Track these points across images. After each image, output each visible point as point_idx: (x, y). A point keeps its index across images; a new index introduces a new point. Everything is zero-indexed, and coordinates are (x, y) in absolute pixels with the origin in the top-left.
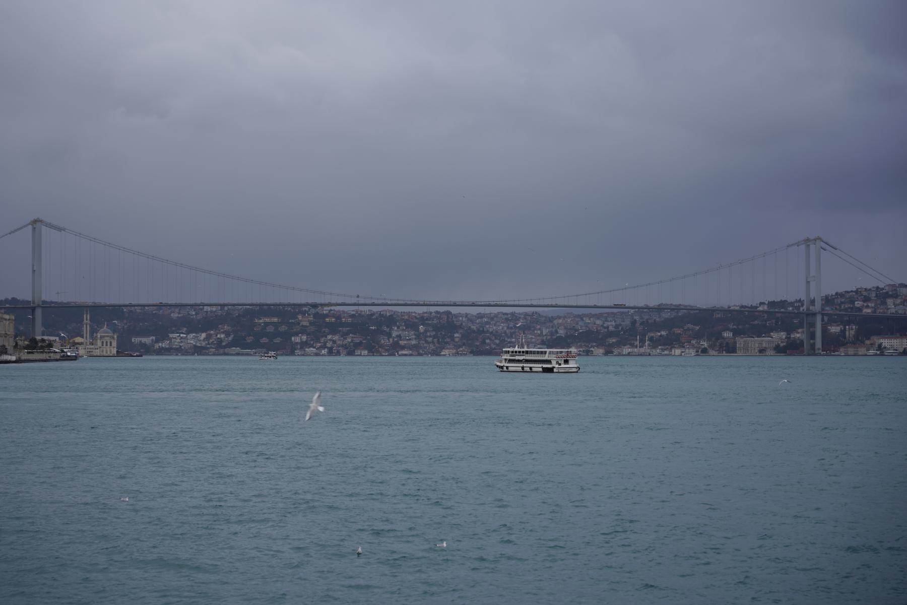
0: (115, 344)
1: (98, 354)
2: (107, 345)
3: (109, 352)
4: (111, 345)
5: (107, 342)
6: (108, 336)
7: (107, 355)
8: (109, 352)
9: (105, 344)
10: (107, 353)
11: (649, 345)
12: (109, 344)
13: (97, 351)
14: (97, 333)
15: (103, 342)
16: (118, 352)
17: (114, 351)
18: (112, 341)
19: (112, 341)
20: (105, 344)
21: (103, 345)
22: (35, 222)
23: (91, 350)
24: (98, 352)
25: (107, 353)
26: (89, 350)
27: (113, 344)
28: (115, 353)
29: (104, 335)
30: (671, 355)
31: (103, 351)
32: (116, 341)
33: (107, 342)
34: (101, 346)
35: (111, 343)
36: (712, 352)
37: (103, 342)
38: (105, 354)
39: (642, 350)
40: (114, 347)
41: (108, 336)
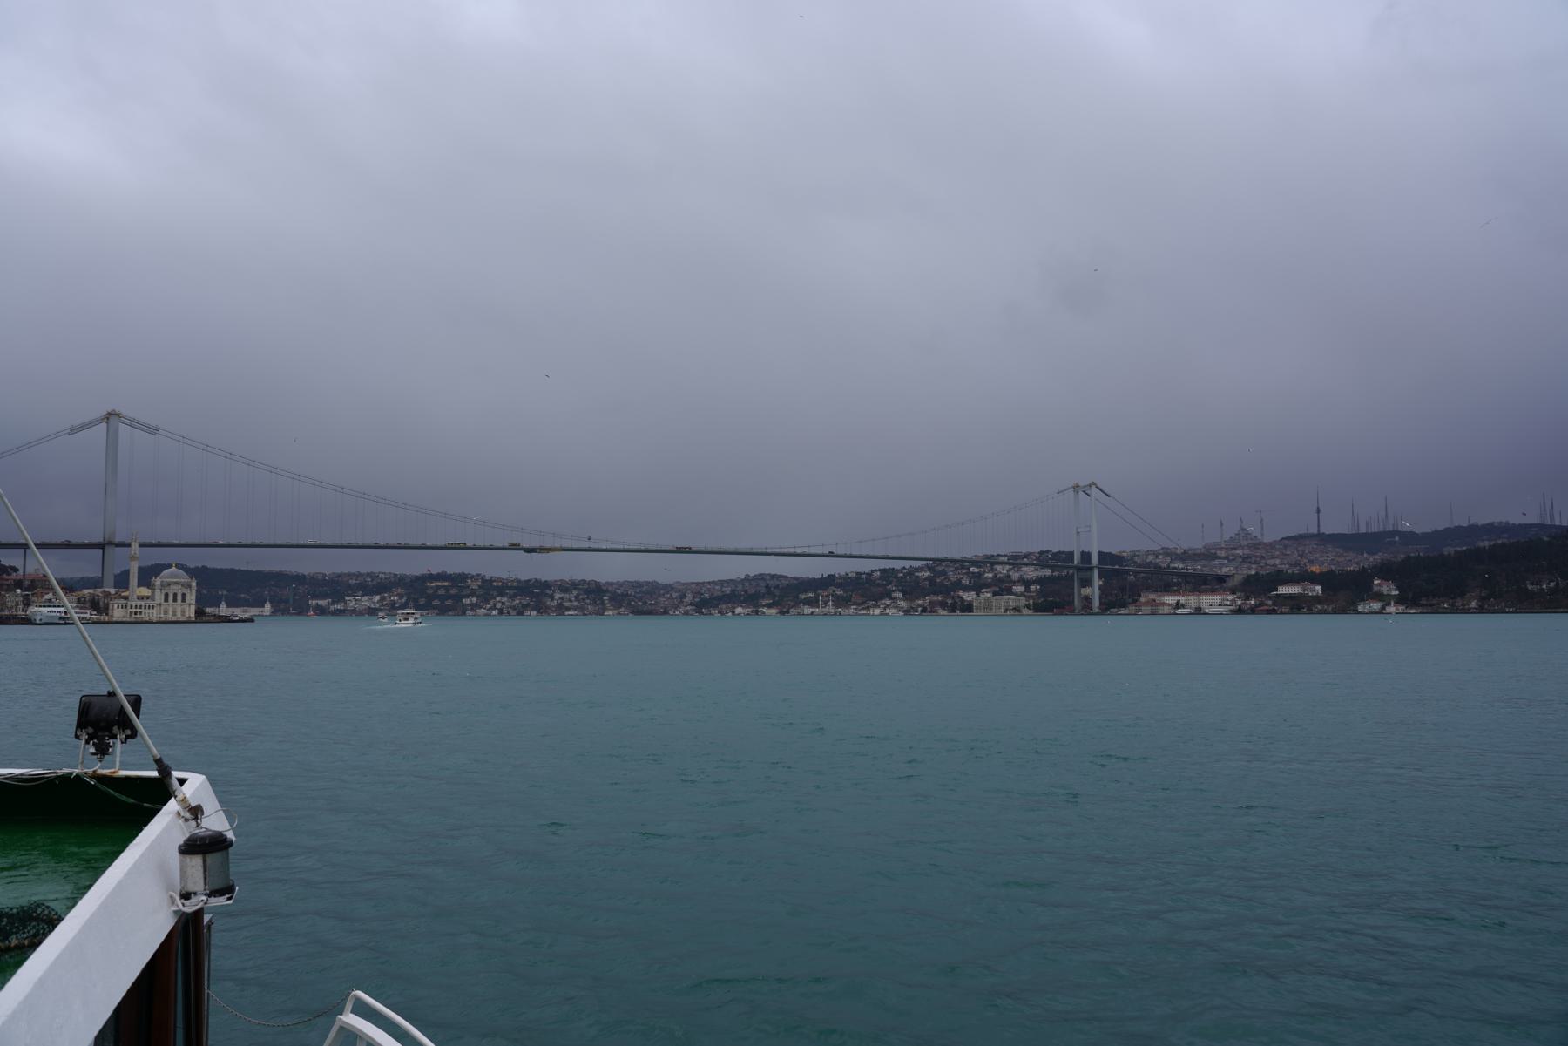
0: (194, 597)
1: (154, 618)
2: (175, 600)
3: (179, 615)
4: (184, 600)
5: (175, 595)
6: (177, 583)
7: (174, 619)
8: (179, 615)
11: (833, 605)
12: (179, 598)
13: (151, 611)
14: (156, 577)
15: (167, 596)
16: (200, 613)
17: (191, 612)
18: (187, 592)
19: (187, 592)
21: (166, 599)
22: (109, 416)
23: (138, 610)
24: (154, 614)
25: (174, 613)
26: (134, 610)
27: (188, 598)
28: (193, 615)
30: (869, 614)
31: (166, 612)
32: (194, 592)
33: (175, 595)
34: (162, 601)
35: (184, 596)
36: (1026, 611)
37: (167, 596)
38: (170, 617)
39: (826, 610)
40: (190, 604)
41: (177, 583)
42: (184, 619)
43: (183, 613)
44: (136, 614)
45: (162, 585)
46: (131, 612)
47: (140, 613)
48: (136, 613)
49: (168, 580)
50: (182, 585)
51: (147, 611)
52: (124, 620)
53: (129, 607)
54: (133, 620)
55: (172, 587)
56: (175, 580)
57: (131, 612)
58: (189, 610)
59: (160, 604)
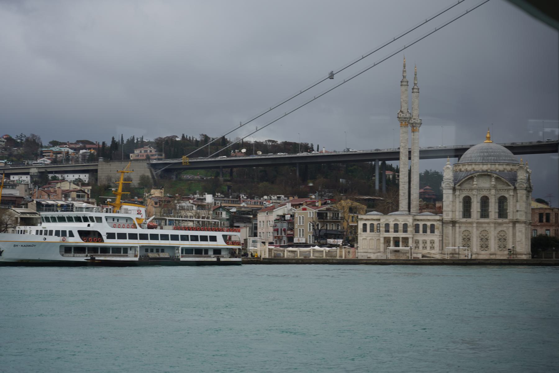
1: (436, 254)
2: (484, 213)
3: (493, 245)
7: (484, 255)
8: (493, 245)
9: (476, 207)
10: (485, 246)
12: (493, 208)
13: (429, 237)
15: (467, 202)
20: (476, 207)
21: (467, 212)
23: (401, 235)
25: (485, 246)
26: (392, 235)
29: (478, 168)
31: (467, 241)
34: (458, 215)
37: (467, 202)
40: (515, 223)
41: (486, 175)
42: (503, 255)
43: (502, 240)
44: (397, 244)
45: (456, 180)
46: (387, 241)
47: (406, 240)
48: (397, 244)
49: (469, 168)
50: (497, 179)
51: (421, 237)
52: (373, 257)
53: (382, 229)
54: (390, 257)
55: (475, 182)
56: (485, 167)
57: (387, 241)
58: (514, 235)
59: (454, 223)
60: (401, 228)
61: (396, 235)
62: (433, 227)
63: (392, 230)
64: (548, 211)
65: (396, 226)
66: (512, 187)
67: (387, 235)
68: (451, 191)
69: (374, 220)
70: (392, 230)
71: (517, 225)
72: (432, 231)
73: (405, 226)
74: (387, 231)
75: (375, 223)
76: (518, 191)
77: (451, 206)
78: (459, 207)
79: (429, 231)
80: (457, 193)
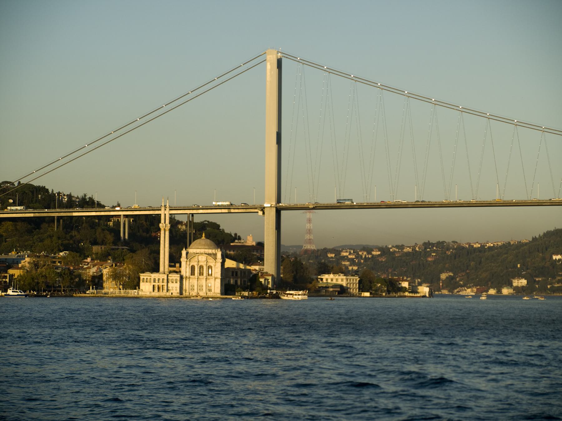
2: (201, 274)
15: (193, 268)
21: (193, 273)
26: (156, 284)
34: (188, 274)
37: (193, 268)
53: (152, 281)
60: (161, 280)
61: (159, 284)
62: (176, 280)
63: (157, 281)
64: (236, 270)
65: (159, 279)
66: (215, 261)
67: (154, 284)
68: (185, 263)
69: (148, 276)
70: (157, 281)
71: (217, 280)
72: (176, 282)
73: (163, 279)
74: (154, 282)
75: (149, 278)
76: (217, 263)
77: (185, 270)
78: (189, 270)
79: (174, 282)
80: (188, 263)
